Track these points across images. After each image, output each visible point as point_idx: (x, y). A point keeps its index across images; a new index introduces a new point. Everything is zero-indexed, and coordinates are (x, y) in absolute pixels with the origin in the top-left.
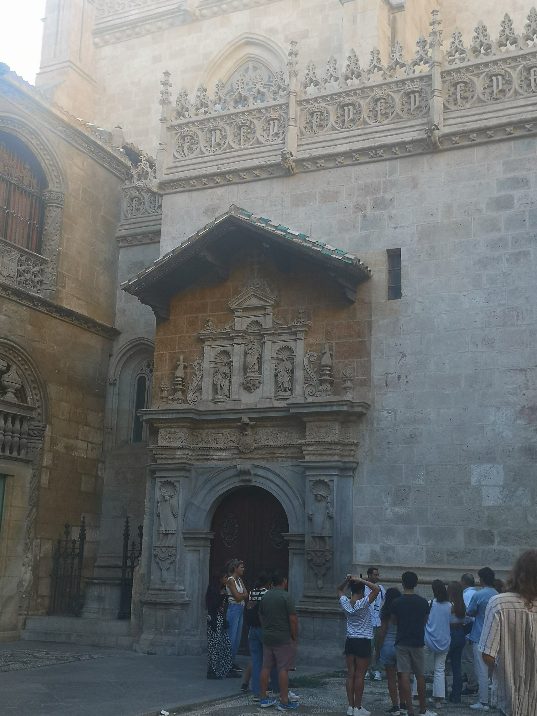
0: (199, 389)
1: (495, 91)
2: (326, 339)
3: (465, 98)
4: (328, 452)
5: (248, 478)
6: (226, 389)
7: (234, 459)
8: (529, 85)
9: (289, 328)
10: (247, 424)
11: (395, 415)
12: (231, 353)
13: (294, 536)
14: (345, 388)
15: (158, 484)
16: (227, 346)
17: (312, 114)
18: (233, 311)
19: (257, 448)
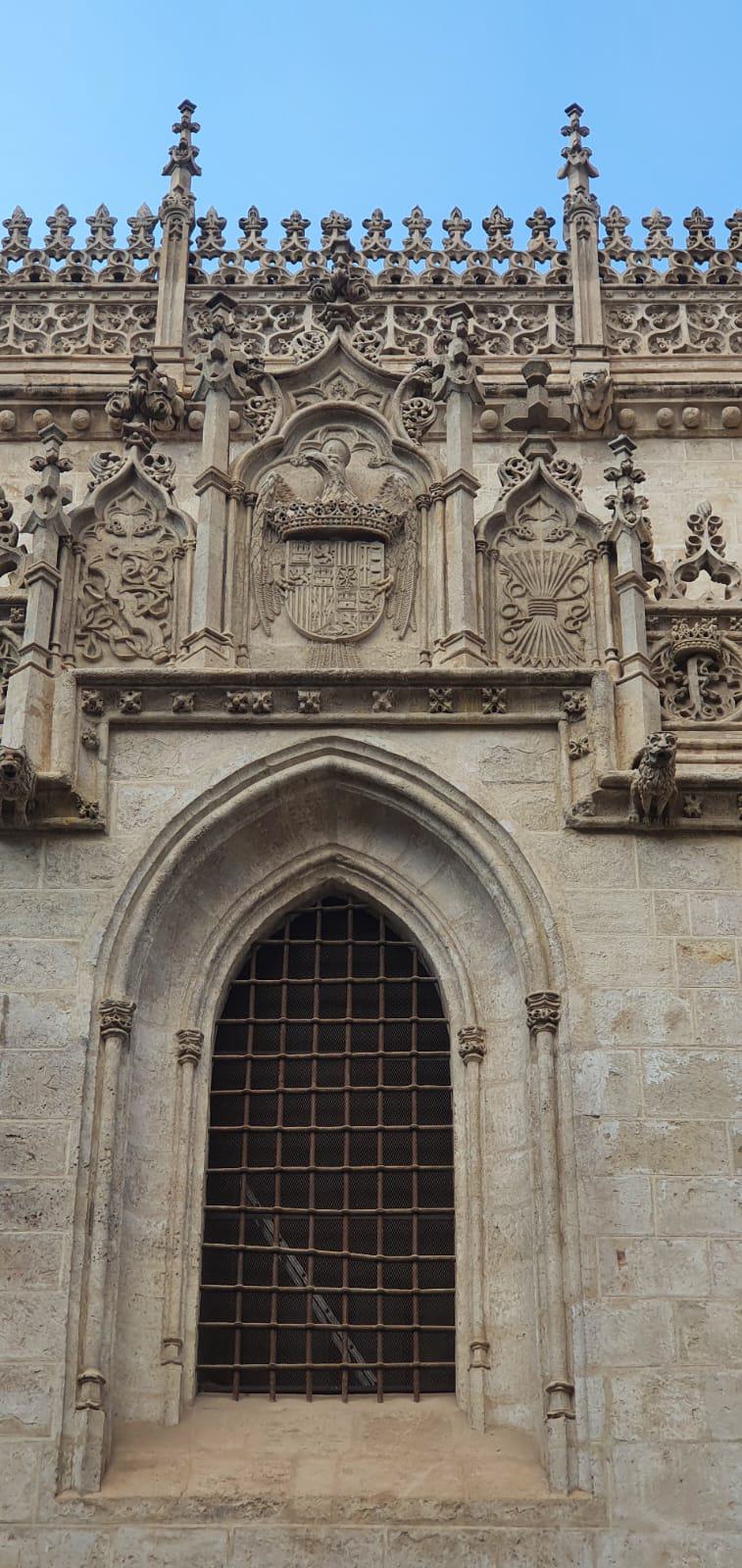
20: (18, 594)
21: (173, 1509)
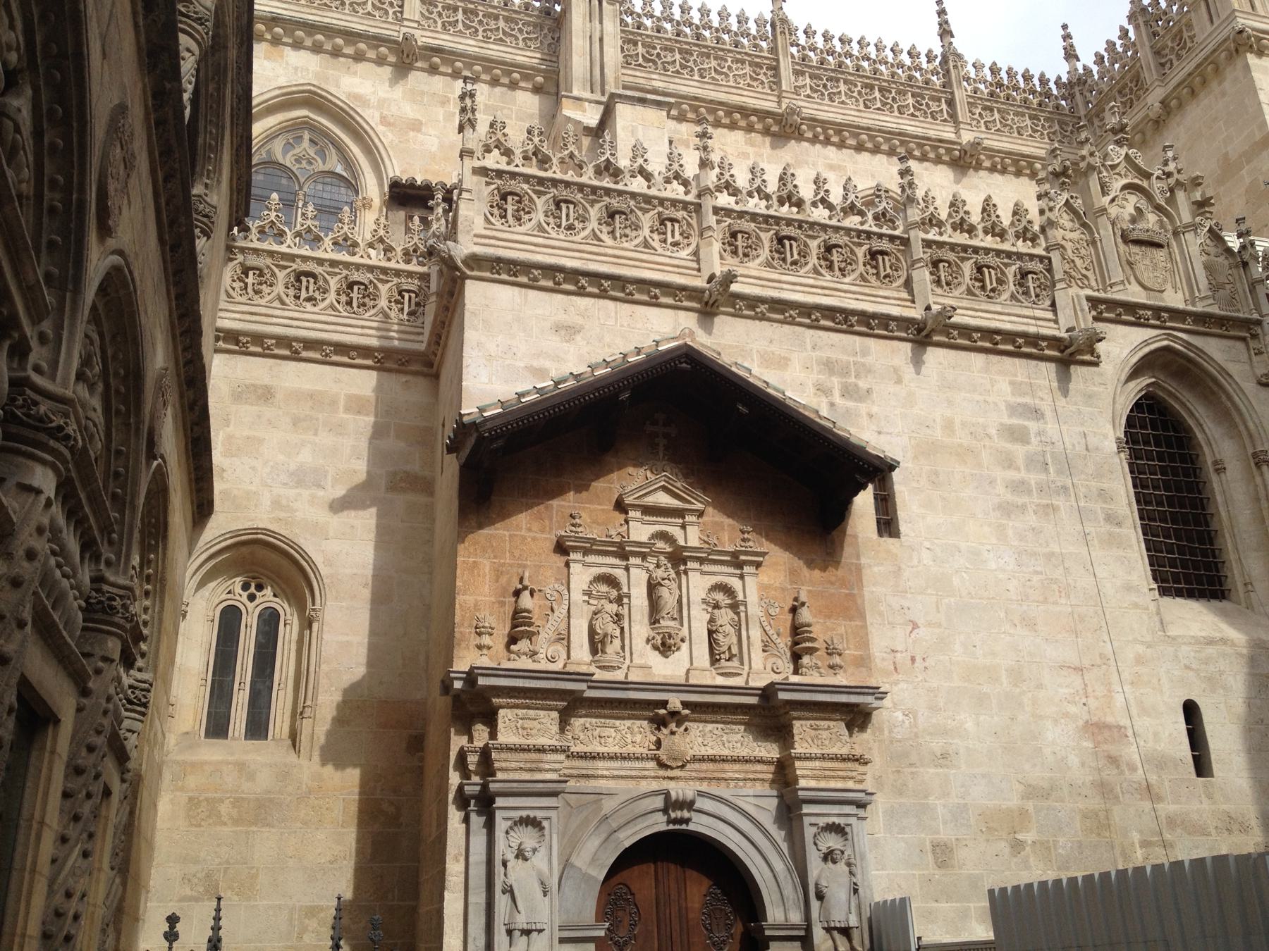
0: (565, 638)
1: (989, 287)
2: (792, 582)
3: (948, 284)
4: (840, 773)
5: (686, 814)
6: (617, 642)
7: (645, 777)
8: (1026, 293)
9: (735, 555)
10: (674, 714)
11: (915, 718)
12: (623, 580)
13: (780, 927)
14: (831, 667)
15: (501, 825)
16: (613, 566)
17: (734, 235)
18: (621, 507)
19: (695, 759)
20: (1044, 253)
21: (1196, 641)
